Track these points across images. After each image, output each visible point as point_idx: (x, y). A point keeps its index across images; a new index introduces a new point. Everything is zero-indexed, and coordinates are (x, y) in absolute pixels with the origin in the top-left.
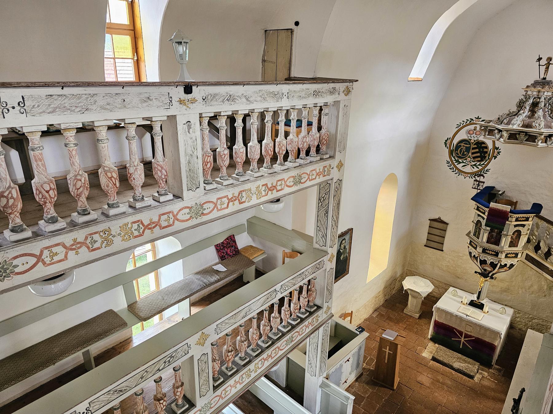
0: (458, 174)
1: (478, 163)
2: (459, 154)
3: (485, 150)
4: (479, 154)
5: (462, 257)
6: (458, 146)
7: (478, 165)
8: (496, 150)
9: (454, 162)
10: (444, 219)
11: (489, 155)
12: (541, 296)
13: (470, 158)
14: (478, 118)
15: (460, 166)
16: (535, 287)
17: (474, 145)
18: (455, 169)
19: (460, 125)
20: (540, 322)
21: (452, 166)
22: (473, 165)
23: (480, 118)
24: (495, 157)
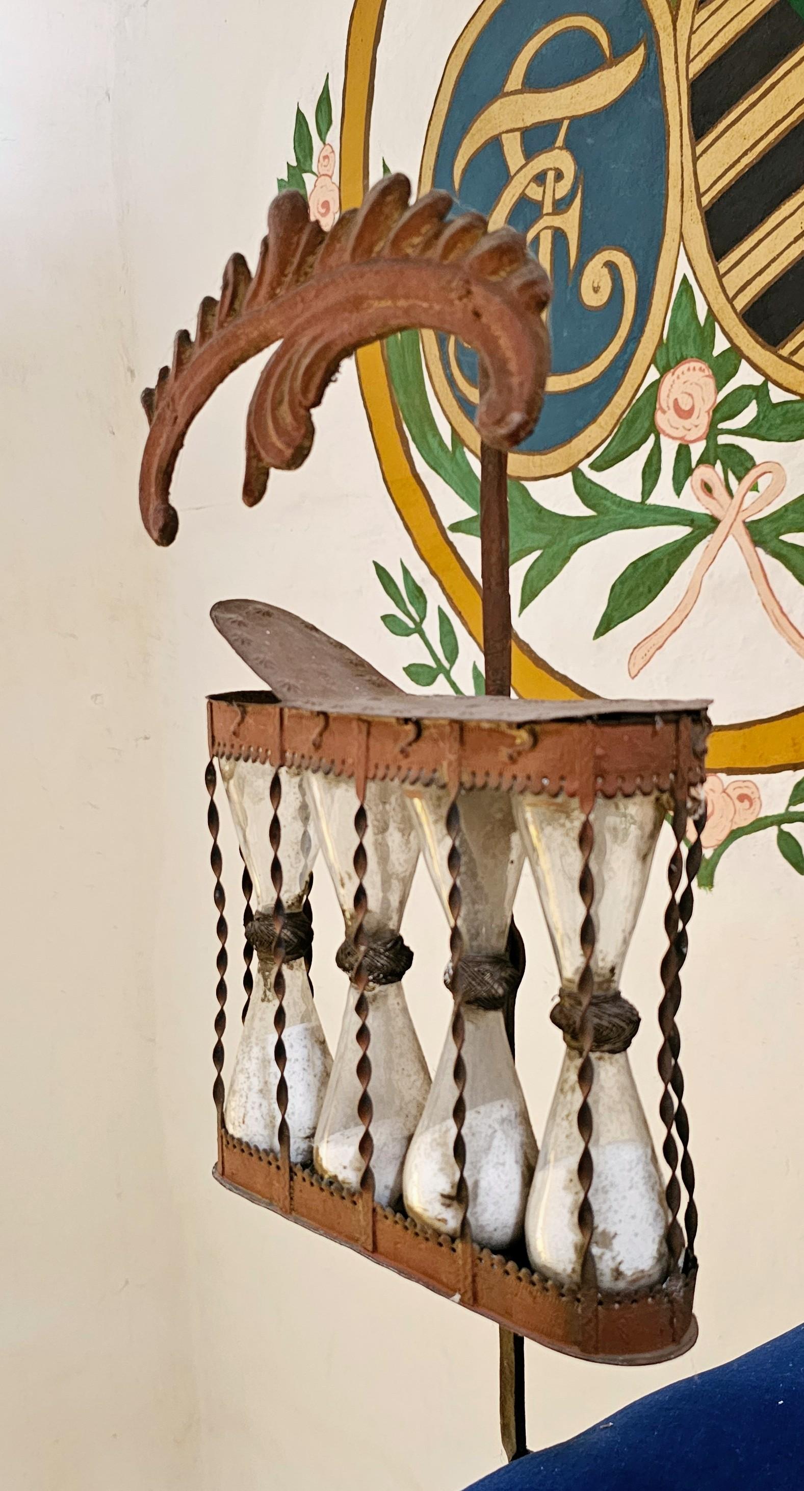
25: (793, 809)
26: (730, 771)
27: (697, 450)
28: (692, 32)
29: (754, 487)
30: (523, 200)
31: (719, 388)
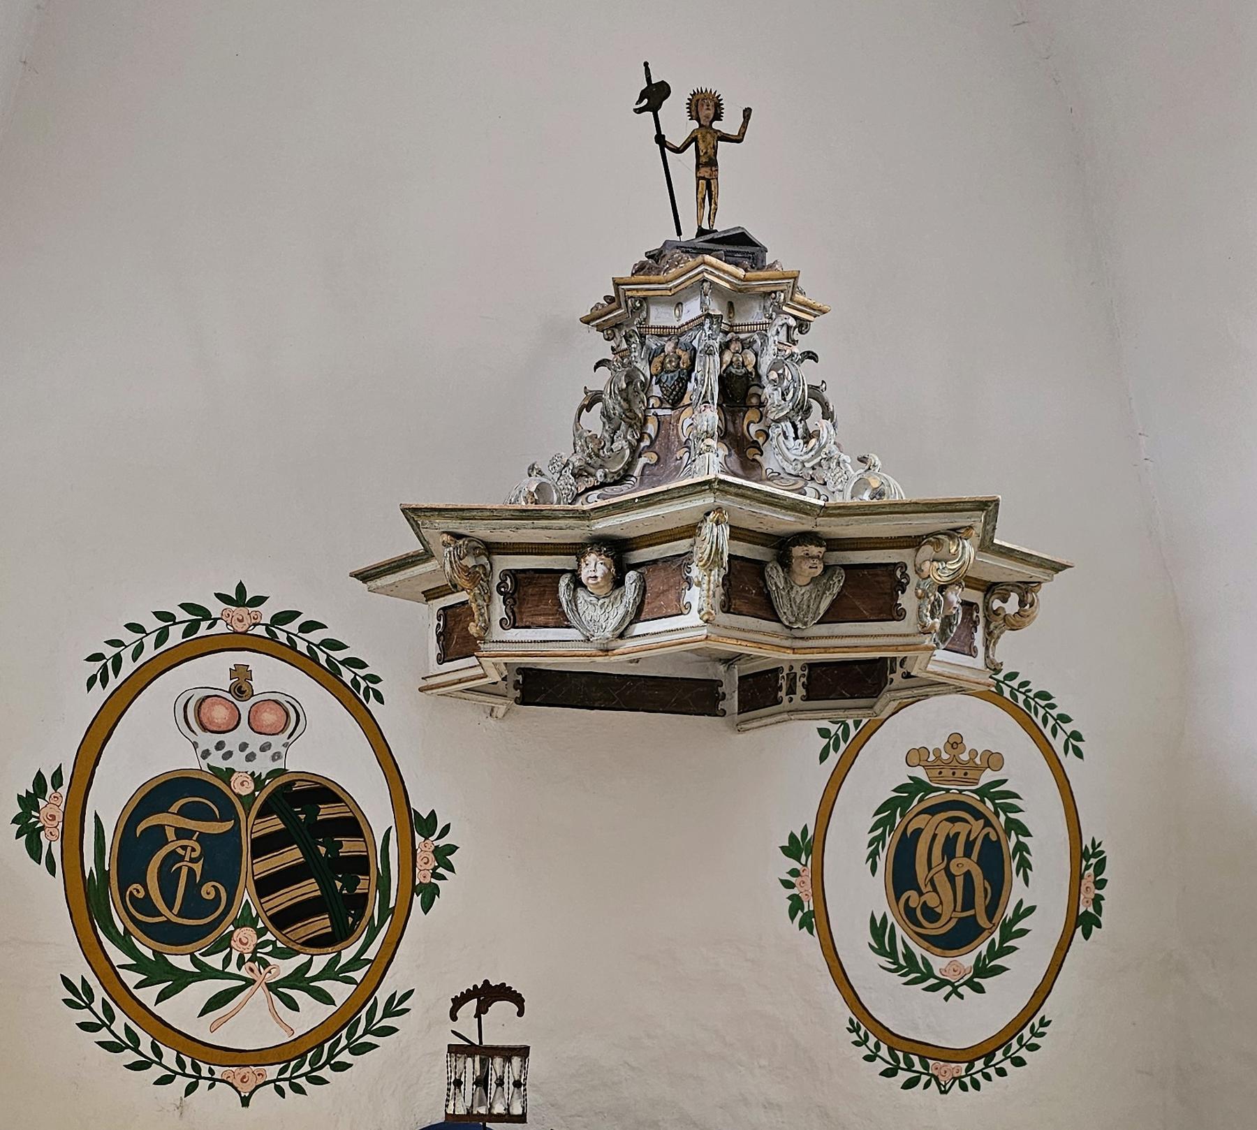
0: (181, 1082)
3: (349, 847)
4: (309, 888)
8: (419, 839)
9: (131, 978)
11: (383, 883)
13: (253, 923)
17: (259, 816)
18: (146, 1041)
21: (121, 1020)
24: (430, 894)
25: (279, 1077)
26: (255, 1066)
28: (253, 825)
29: (270, 972)
30: (174, 852)
31: (258, 939)
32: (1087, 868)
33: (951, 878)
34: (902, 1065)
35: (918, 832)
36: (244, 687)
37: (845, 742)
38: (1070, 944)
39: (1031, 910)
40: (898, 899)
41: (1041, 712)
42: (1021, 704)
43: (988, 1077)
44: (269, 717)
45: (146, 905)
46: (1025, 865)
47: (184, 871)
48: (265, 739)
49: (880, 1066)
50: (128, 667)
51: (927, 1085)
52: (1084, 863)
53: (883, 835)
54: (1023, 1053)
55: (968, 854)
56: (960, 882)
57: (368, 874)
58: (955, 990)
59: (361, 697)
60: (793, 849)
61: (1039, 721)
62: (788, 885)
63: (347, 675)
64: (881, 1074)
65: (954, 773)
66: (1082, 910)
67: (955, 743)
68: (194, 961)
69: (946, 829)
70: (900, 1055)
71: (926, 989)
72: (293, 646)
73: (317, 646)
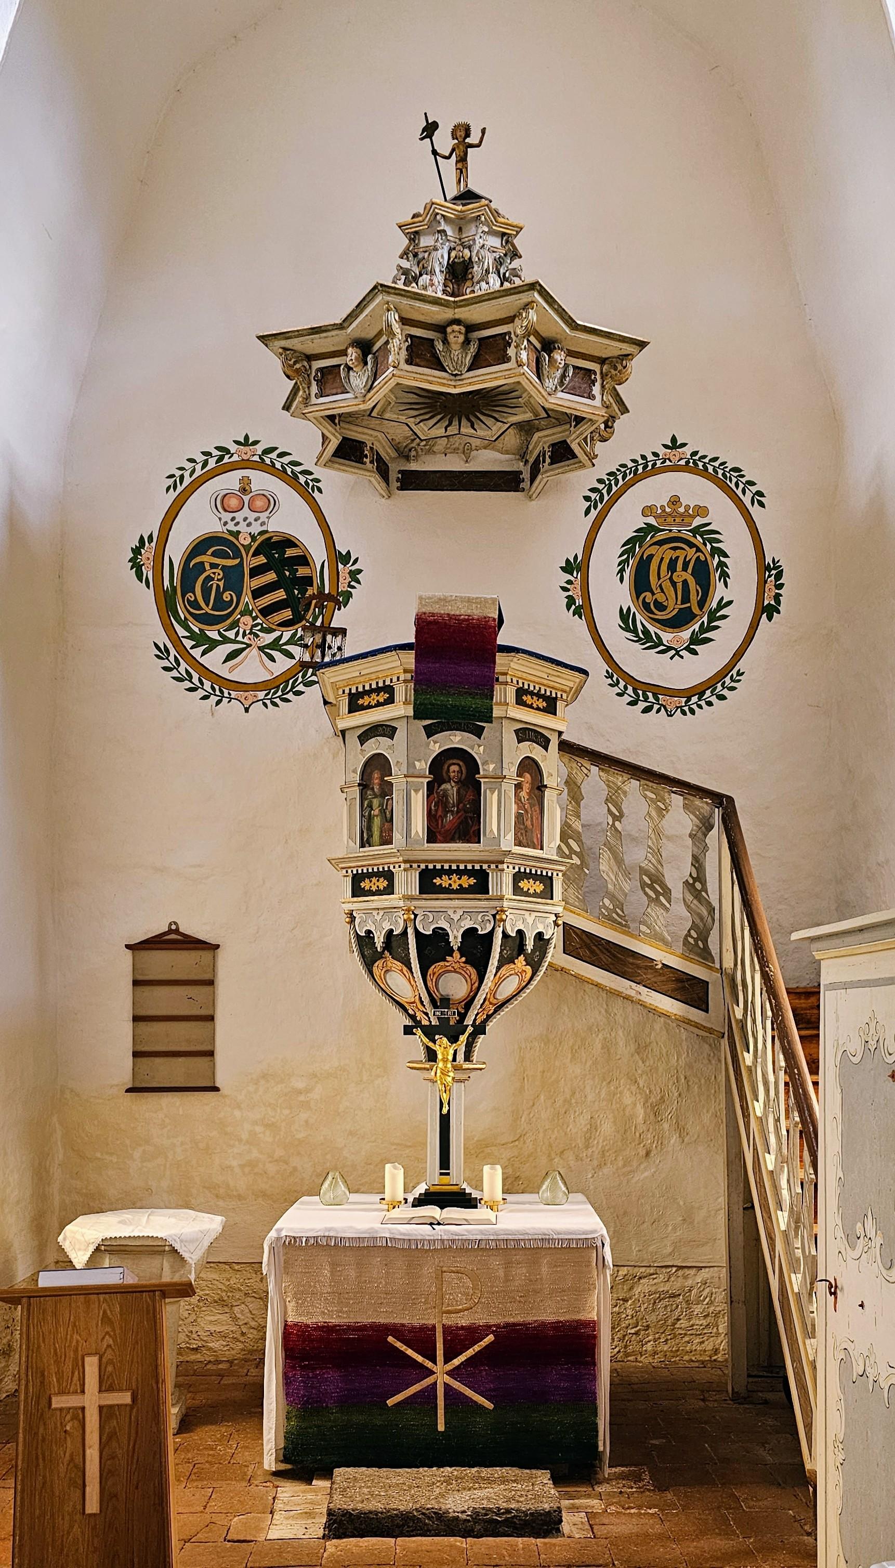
0: (214, 699)
1: (287, 636)
2: (203, 604)
3: (302, 571)
4: (281, 594)
5: (308, 1090)
6: (190, 572)
7: (285, 644)
8: (341, 566)
9: (188, 643)
10: (190, 928)
12: (635, 1164)
14: (246, 442)
15: (214, 660)
16: (607, 1128)
17: (253, 556)
18: (195, 677)
19: (182, 477)
20: (660, 1283)
21: (183, 665)
22: (269, 646)
23: (256, 443)
27: (248, 632)
32: (770, 576)
33: (674, 584)
34: (641, 698)
35: (651, 557)
36: (247, 488)
37: (601, 503)
38: (758, 625)
39: (730, 603)
40: (638, 598)
41: (734, 480)
42: (720, 476)
43: (700, 707)
44: (259, 503)
45: (195, 604)
46: (725, 576)
47: (214, 587)
48: (257, 515)
49: (626, 699)
50: (187, 481)
51: (658, 711)
52: (767, 573)
53: (628, 559)
54: (725, 692)
55: (685, 569)
56: (679, 586)
57: (312, 586)
58: (677, 653)
59: (310, 491)
60: (568, 568)
61: (733, 486)
62: (565, 589)
63: (302, 479)
64: (628, 704)
65: (674, 520)
66: (766, 603)
67: (675, 501)
68: (220, 633)
69: (669, 555)
70: (640, 692)
71: (658, 652)
72: (273, 465)
73: (287, 465)
